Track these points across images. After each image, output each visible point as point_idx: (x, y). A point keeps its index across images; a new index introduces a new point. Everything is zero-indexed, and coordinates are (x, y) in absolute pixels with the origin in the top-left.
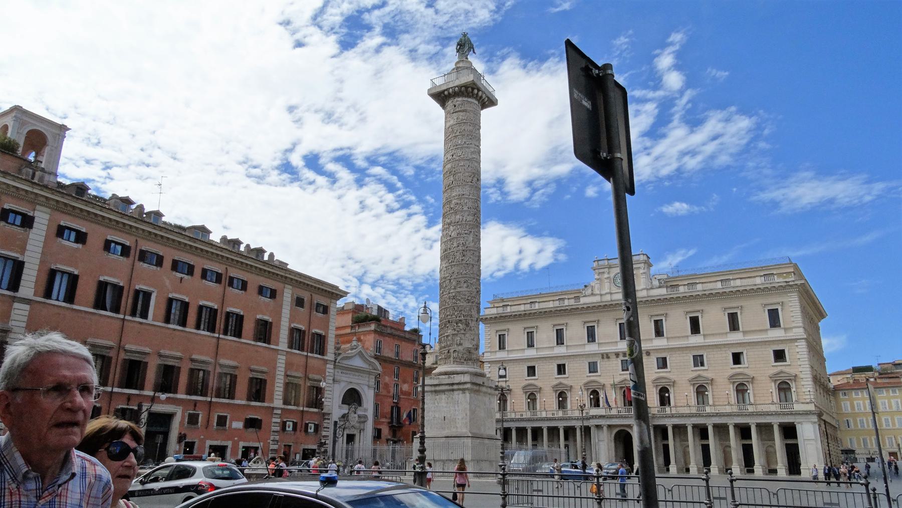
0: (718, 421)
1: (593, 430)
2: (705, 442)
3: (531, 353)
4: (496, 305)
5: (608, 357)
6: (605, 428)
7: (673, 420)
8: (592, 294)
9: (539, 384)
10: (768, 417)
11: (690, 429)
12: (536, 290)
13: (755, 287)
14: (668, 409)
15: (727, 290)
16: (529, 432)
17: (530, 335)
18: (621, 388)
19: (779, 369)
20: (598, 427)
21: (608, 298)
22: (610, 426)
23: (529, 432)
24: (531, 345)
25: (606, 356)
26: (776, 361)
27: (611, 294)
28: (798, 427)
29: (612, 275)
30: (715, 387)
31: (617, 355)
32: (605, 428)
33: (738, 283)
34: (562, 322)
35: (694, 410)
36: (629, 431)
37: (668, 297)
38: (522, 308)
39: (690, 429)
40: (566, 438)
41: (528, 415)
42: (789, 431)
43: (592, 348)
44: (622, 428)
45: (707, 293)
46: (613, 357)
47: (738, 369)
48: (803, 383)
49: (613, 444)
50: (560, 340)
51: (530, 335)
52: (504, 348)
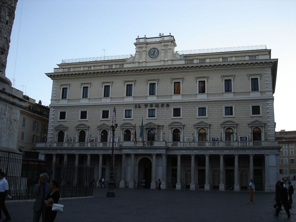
0: (212, 152)
1: (124, 157)
2: (230, 168)
3: (85, 102)
4: (63, 67)
5: (140, 107)
6: (133, 156)
7: (181, 151)
8: (133, 63)
9: (87, 124)
10: (247, 151)
11: (193, 158)
12: (94, 58)
13: (245, 63)
14: (179, 143)
15: (226, 64)
16: (77, 157)
17: (85, 89)
18: (147, 129)
19: (255, 119)
20: (128, 155)
21: (144, 65)
22: (136, 155)
23: (77, 157)
24: (85, 95)
25: (138, 106)
26: (253, 114)
27: (146, 62)
28: (266, 157)
29: (148, 49)
30: (211, 130)
31: (146, 105)
32: (133, 156)
33: (234, 59)
34: (108, 81)
35: (196, 145)
36: (150, 158)
37: (186, 66)
38: (82, 69)
39: (193, 158)
40: (104, 163)
41: (77, 145)
42: (260, 160)
43: (129, 100)
44: (145, 157)
45: (213, 64)
46: (143, 107)
47: (229, 118)
48: (269, 129)
49: (137, 168)
50: (107, 94)
51: (85, 89)
52: (65, 98)
